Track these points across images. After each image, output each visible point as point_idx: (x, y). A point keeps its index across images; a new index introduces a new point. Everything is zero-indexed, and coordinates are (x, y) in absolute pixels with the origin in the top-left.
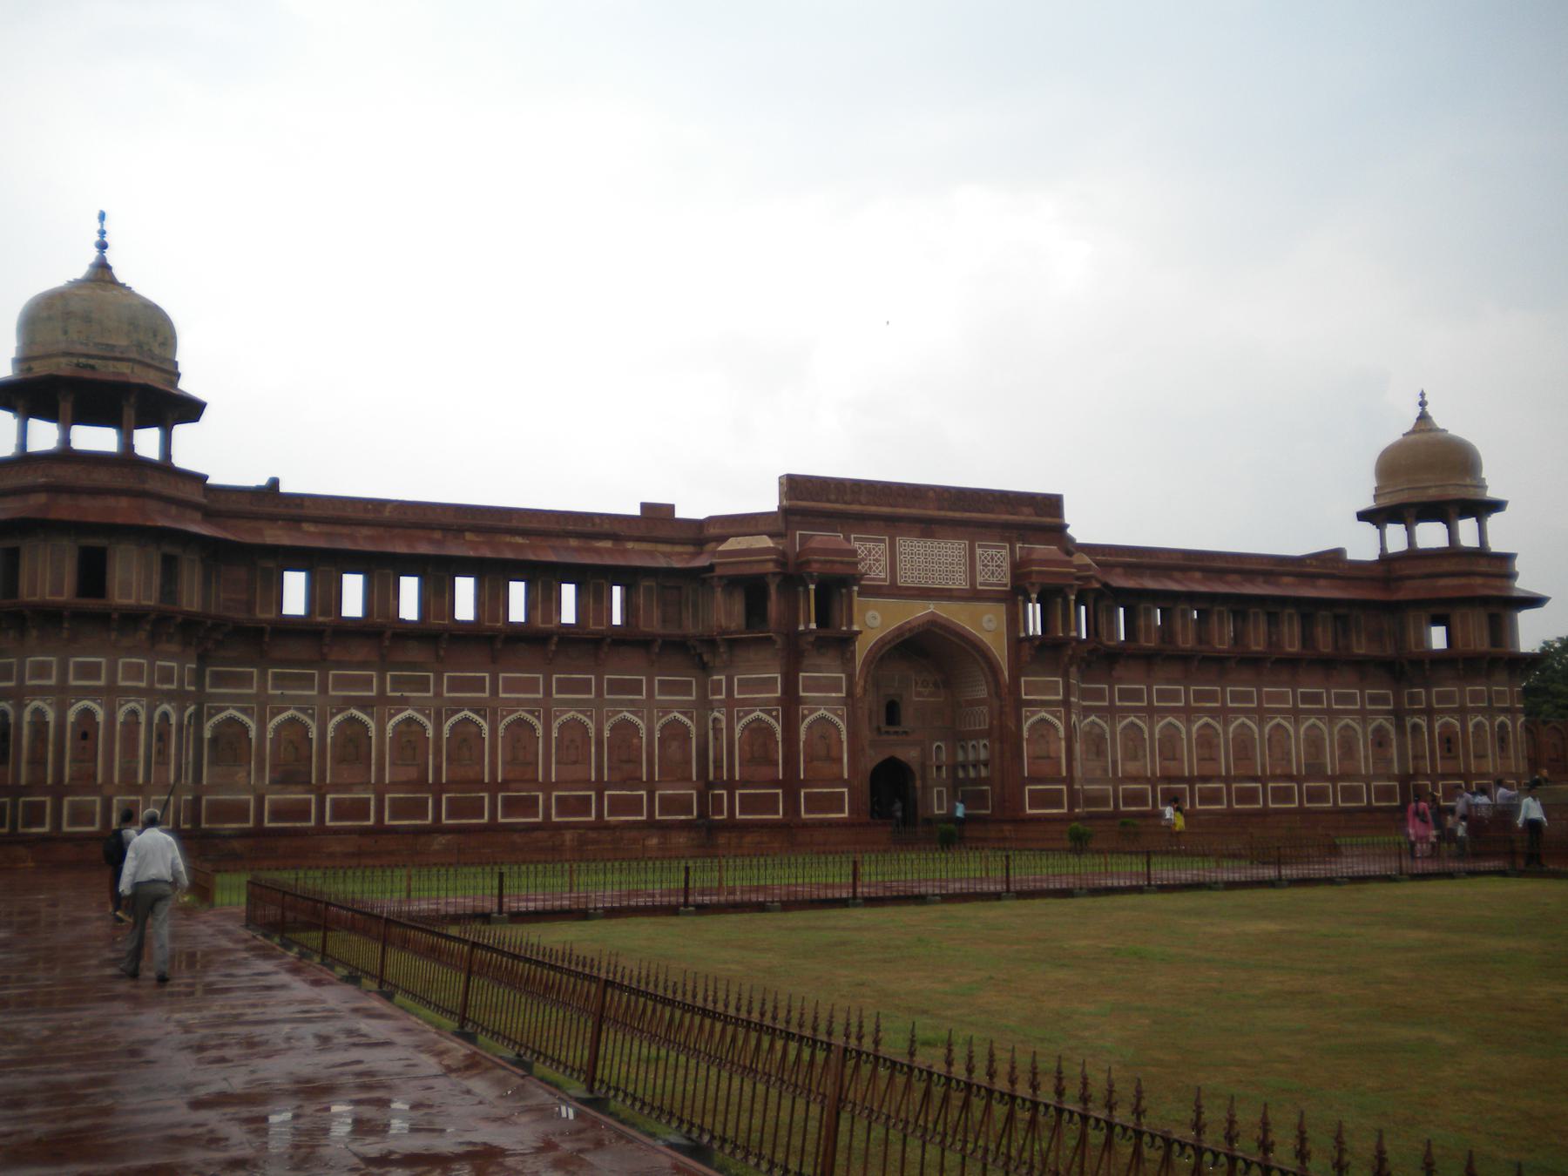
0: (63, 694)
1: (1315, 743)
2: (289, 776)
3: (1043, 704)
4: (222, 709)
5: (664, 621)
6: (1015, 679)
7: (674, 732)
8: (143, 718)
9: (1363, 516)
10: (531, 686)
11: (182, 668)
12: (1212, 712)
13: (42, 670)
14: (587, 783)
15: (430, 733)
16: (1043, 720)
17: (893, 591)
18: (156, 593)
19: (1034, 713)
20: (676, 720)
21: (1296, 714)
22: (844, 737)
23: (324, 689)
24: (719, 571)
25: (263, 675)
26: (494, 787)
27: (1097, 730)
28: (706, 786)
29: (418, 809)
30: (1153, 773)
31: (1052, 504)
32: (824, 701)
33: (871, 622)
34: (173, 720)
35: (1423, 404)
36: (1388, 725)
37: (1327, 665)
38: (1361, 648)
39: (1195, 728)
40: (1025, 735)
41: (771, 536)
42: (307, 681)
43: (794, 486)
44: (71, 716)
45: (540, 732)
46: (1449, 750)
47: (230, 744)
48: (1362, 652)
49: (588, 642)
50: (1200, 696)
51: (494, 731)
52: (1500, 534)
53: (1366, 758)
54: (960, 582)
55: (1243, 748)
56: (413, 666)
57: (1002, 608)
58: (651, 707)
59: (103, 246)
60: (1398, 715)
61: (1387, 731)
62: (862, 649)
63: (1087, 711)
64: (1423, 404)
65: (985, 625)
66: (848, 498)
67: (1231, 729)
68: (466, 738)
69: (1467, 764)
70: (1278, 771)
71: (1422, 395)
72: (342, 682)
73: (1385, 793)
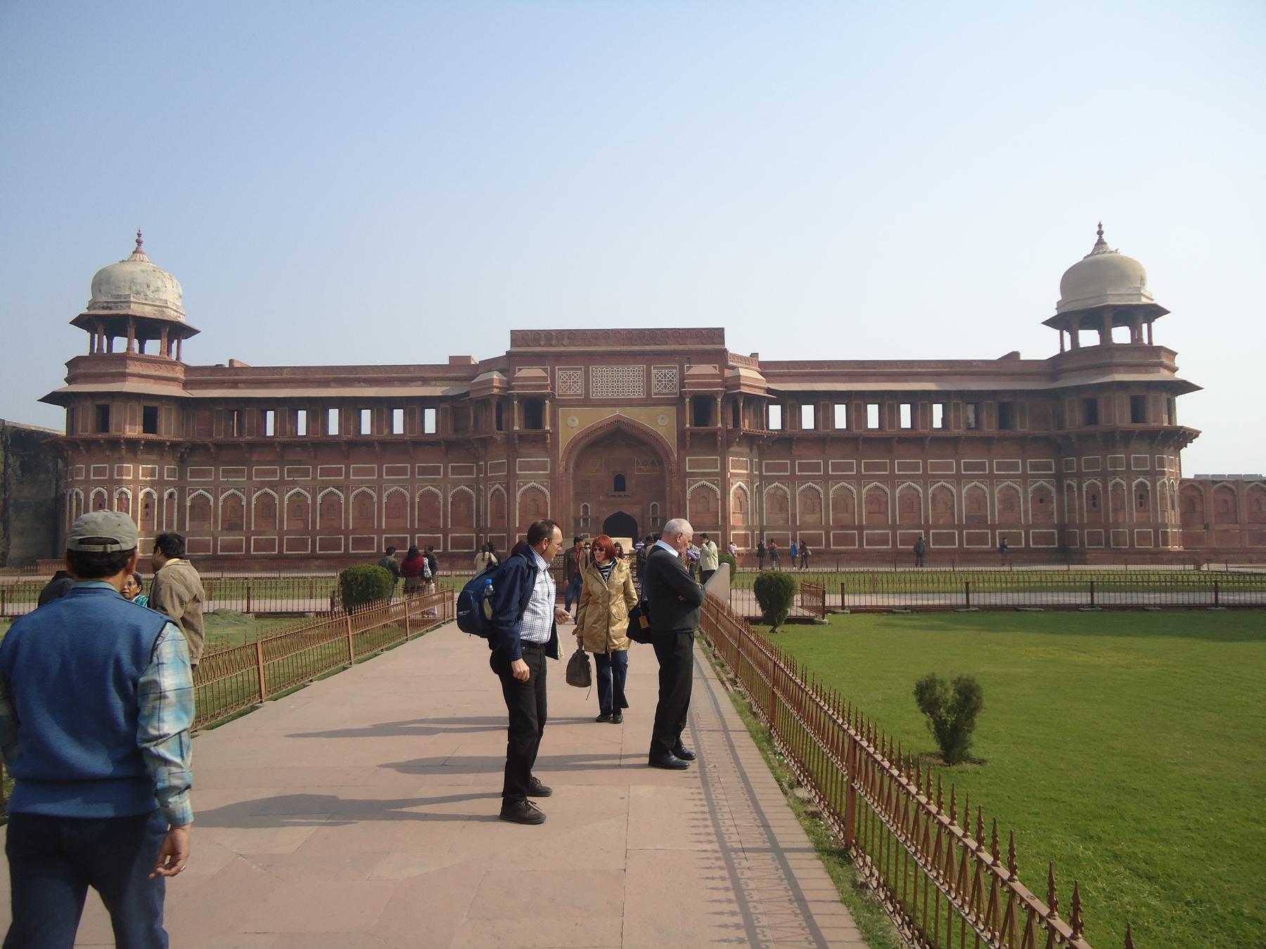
0: (88, 484)
1: (978, 501)
2: (231, 526)
3: (703, 475)
4: (195, 490)
5: (456, 430)
6: (681, 460)
7: (461, 498)
8: (130, 497)
9: (1050, 323)
10: (370, 472)
11: (161, 469)
12: (879, 478)
13: (79, 472)
14: (404, 530)
15: (310, 501)
16: (704, 486)
17: (586, 402)
18: (139, 428)
19: (697, 481)
20: (462, 490)
21: (958, 479)
22: (548, 500)
23: (250, 478)
24: (472, 396)
25: (217, 470)
26: (347, 533)
27: (780, 492)
28: (480, 529)
29: (303, 545)
30: (827, 522)
31: (718, 334)
32: (534, 477)
33: (569, 422)
34: (155, 496)
35: (1100, 233)
36: (1049, 486)
37: (988, 442)
38: (1022, 427)
39: (864, 491)
40: (688, 496)
41: (501, 371)
42: (239, 473)
43: (518, 337)
44: (92, 496)
45: (375, 499)
46: (1094, 505)
47: (201, 509)
48: (1026, 430)
49: (415, 443)
50: (869, 467)
51: (347, 500)
52: (1160, 333)
53: (1026, 511)
54: (638, 393)
55: (910, 504)
56: (300, 462)
57: (674, 409)
58: (444, 484)
59: (139, 242)
60: (1059, 479)
61: (1049, 492)
62: (564, 441)
63: (771, 480)
64: (1100, 233)
65: (662, 424)
66: (554, 342)
67: (898, 491)
68: (330, 505)
69: (1107, 515)
70: (941, 522)
71: (1100, 226)
72: (259, 473)
73: (1048, 538)
